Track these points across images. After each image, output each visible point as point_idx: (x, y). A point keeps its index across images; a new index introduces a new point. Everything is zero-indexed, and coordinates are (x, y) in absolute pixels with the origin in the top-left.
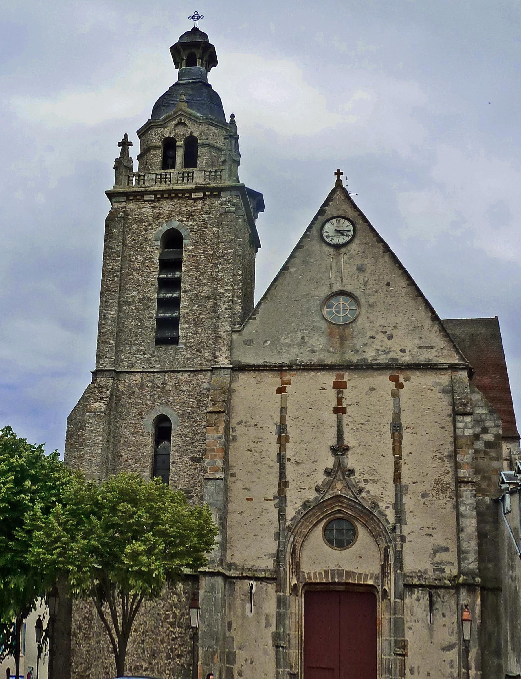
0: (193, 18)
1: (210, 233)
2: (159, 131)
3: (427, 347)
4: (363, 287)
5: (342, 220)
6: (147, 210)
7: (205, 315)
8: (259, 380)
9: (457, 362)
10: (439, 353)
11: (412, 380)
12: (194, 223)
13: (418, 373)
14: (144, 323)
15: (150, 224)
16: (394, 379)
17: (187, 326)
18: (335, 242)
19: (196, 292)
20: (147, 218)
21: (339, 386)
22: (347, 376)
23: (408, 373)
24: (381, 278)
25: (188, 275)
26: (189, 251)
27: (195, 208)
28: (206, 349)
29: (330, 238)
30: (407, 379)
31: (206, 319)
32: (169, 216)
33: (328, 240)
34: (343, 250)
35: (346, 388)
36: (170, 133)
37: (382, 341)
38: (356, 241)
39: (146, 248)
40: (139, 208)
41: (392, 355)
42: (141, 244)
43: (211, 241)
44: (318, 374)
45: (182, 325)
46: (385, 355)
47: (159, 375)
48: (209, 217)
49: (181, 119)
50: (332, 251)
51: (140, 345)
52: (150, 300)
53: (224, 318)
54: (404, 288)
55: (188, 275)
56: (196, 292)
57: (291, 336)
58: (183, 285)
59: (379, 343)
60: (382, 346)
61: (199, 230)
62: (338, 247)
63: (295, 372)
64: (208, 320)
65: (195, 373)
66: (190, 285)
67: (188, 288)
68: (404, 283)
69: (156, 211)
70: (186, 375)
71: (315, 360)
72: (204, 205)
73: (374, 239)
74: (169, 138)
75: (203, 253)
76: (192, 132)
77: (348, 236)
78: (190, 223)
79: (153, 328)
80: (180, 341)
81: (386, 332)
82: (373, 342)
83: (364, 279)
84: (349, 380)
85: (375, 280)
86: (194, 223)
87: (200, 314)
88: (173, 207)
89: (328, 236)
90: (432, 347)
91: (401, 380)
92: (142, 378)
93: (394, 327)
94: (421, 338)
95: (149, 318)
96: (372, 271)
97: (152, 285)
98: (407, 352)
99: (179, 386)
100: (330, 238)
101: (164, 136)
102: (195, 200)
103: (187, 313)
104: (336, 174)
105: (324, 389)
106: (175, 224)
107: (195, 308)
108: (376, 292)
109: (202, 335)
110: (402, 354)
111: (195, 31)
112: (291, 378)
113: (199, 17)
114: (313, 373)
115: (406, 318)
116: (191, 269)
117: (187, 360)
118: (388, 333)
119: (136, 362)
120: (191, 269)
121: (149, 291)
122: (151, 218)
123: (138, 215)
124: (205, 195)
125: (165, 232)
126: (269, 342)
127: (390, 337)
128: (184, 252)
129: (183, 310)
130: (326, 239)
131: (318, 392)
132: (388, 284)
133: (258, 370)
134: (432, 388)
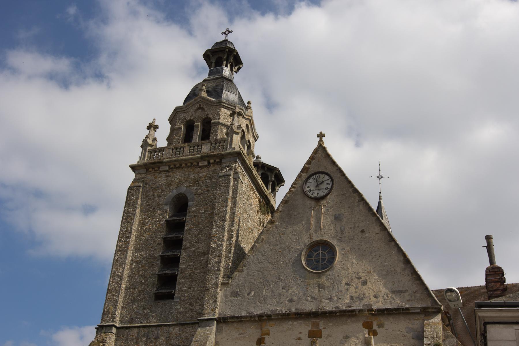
0: (225, 33)
1: (210, 196)
2: (182, 116)
3: (400, 292)
4: (340, 235)
5: (322, 176)
6: (162, 179)
7: (199, 269)
8: (241, 332)
9: (429, 305)
10: (411, 297)
11: (386, 326)
12: (198, 188)
13: (391, 319)
14: (147, 280)
15: (163, 191)
16: (368, 326)
17: (183, 281)
18: (316, 195)
19: (194, 249)
20: (161, 185)
21: (315, 335)
22: (322, 325)
23: (382, 319)
24: (357, 225)
25: (189, 234)
26: (192, 212)
27: (201, 175)
28: (197, 302)
29: (312, 192)
30: (380, 326)
31: (200, 273)
32: (179, 183)
33: (310, 194)
34: (323, 202)
35: (321, 337)
36: (191, 117)
37: (356, 288)
38: (334, 193)
39: (157, 212)
40: (156, 178)
41: (366, 301)
42: (154, 209)
43: (211, 202)
44: (295, 323)
45: (180, 280)
46: (359, 302)
47: (154, 329)
48: (211, 181)
49: (200, 105)
50: (313, 203)
51: (141, 300)
52: (155, 258)
53: (214, 271)
54: (377, 234)
55: (189, 234)
56: (194, 249)
57: (273, 286)
58: (184, 243)
59: (354, 290)
60: (356, 292)
61: (202, 193)
62: (318, 200)
63: (273, 322)
64: (202, 274)
65: (186, 326)
66: (189, 242)
67: (188, 245)
68: (377, 229)
69: (169, 179)
70: (177, 329)
71: (294, 310)
72: (209, 171)
73: (351, 190)
74: (190, 120)
75: (204, 213)
76: (208, 114)
77: (327, 189)
78: (196, 188)
79: (154, 284)
80: (176, 295)
81: (361, 278)
82: (347, 290)
83: (341, 228)
84: (324, 328)
85: (351, 228)
86: (198, 188)
87: (196, 269)
88: (183, 175)
89: (310, 191)
90: (406, 291)
91: (375, 327)
92: (138, 333)
93: (368, 272)
94: (394, 283)
95: (152, 275)
96: (348, 219)
97: (158, 244)
98: (381, 299)
99: (170, 339)
100: (312, 192)
101: (185, 119)
102: (201, 167)
103: (185, 268)
104: (318, 136)
105: (300, 339)
106: (183, 189)
107: (191, 263)
108: (352, 239)
109: (196, 289)
110: (375, 299)
111: (226, 41)
112: (270, 328)
113: (229, 32)
114: (290, 323)
115: (379, 263)
116: (191, 228)
117: (180, 314)
118: (363, 279)
119: (136, 318)
120: (191, 228)
121: (155, 250)
122: (164, 186)
123: (154, 184)
124: (209, 163)
125: (175, 197)
126: (253, 293)
127: (365, 283)
128: (188, 213)
129: (182, 266)
130: (308, 193)
131: (294, 342)
132: (363, 231)
133: (241, 321)
134: (406, 334)
